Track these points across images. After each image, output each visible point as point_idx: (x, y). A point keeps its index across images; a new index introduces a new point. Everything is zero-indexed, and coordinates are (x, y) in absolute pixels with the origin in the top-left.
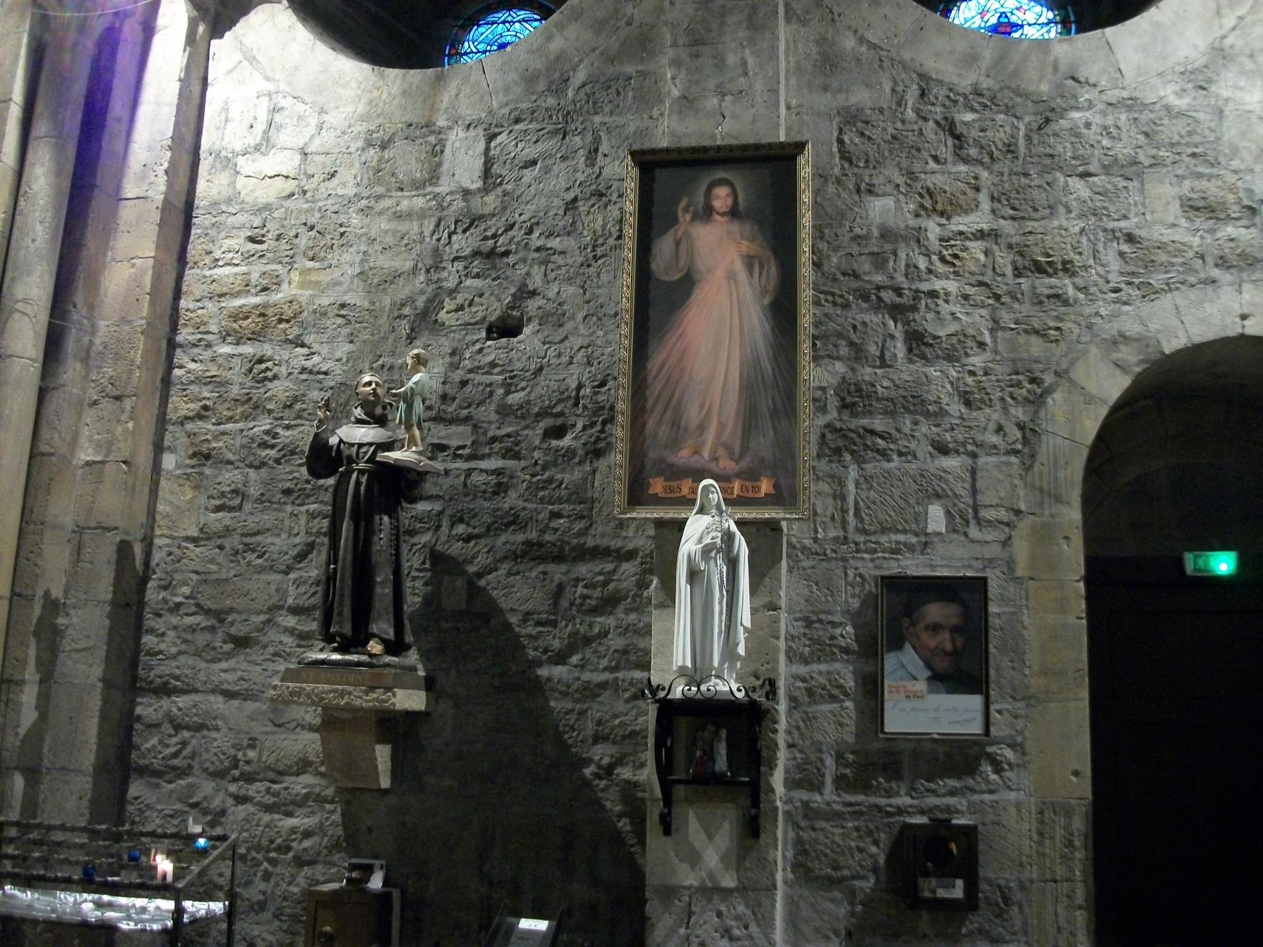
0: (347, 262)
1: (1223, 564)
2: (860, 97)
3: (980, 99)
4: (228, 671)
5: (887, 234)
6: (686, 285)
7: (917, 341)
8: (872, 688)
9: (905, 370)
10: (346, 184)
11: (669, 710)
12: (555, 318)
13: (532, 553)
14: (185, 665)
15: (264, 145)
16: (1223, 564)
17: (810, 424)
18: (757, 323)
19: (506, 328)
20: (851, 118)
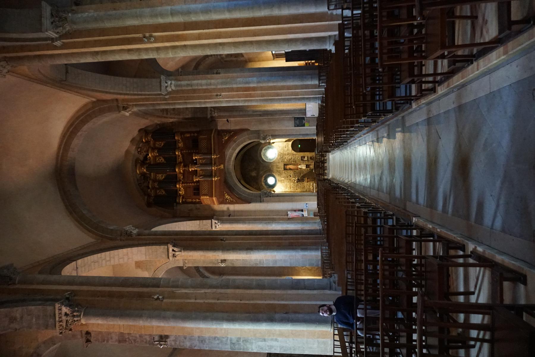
0: (288, 184)
1: (299, 146)
2: (280, 161)
3: (281, 156)
4: (306, 187)
5: (287, 160)
6: (290, 168)
7: (291, 159)
8: (305, 161)
9: (292, 159)
10: (283, 184)
11: (306, 168)
12: (290, 174)
13: (300, 174)
14: (305, 189)
15: (281, 188)
16: (299, 146)
17: (295, 163)
18: (291, 165)
19: (291, 176)
20: (281, 162)
